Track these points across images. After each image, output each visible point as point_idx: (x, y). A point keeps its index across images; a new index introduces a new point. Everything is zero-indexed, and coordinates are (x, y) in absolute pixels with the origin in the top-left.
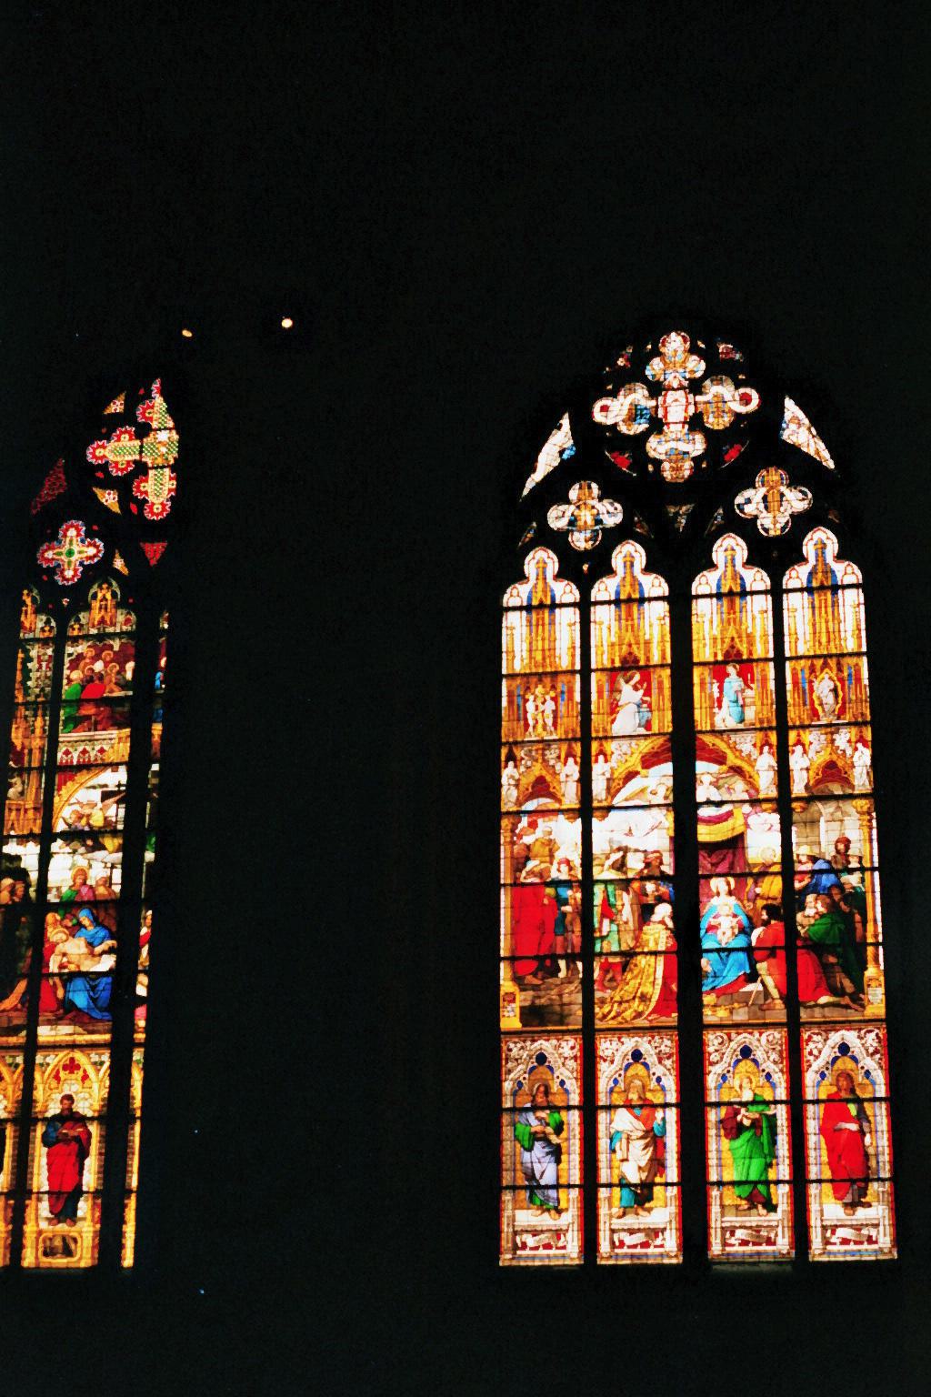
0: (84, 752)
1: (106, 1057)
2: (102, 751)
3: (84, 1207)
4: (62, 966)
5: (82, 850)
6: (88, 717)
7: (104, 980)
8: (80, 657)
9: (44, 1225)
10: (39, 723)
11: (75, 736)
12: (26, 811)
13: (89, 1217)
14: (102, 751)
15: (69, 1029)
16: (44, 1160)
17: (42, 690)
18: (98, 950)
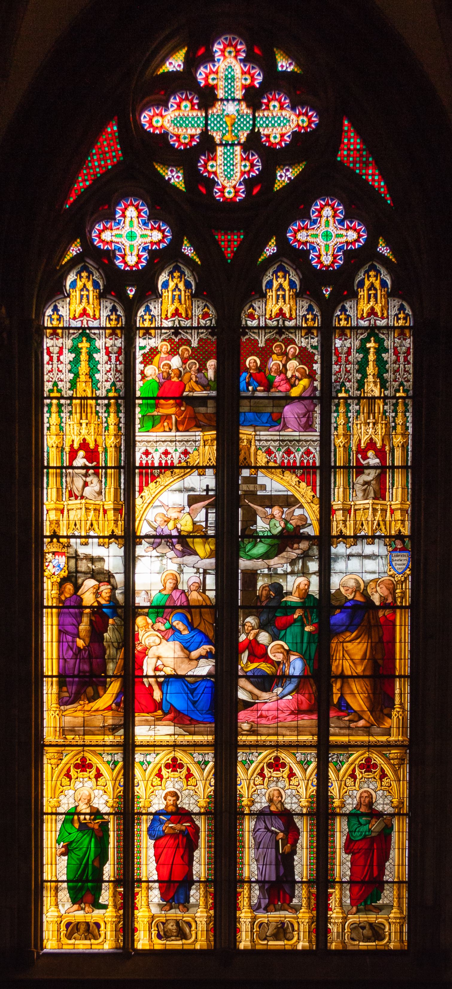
0: (166, 453)
1: (210, 757)
2: (186, 453)
3: (196, 895)
4: (156, 669)
5: (171, 554)
6: (168, 417)
7: (204, 684)
8: (154, 352)
9: (155, 910)
10: (112, 419)
11: (153, 436)
12: (105, 512)
13: (202, 903)
14: (186, 453)
15: (170, 729)
16: (152, 852)
17: (114, 384)
18: (195, 654)
